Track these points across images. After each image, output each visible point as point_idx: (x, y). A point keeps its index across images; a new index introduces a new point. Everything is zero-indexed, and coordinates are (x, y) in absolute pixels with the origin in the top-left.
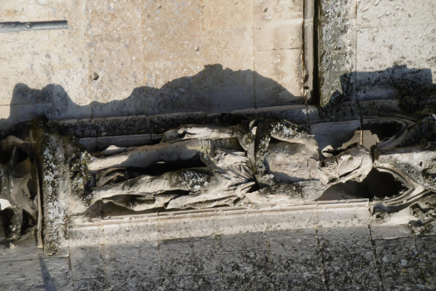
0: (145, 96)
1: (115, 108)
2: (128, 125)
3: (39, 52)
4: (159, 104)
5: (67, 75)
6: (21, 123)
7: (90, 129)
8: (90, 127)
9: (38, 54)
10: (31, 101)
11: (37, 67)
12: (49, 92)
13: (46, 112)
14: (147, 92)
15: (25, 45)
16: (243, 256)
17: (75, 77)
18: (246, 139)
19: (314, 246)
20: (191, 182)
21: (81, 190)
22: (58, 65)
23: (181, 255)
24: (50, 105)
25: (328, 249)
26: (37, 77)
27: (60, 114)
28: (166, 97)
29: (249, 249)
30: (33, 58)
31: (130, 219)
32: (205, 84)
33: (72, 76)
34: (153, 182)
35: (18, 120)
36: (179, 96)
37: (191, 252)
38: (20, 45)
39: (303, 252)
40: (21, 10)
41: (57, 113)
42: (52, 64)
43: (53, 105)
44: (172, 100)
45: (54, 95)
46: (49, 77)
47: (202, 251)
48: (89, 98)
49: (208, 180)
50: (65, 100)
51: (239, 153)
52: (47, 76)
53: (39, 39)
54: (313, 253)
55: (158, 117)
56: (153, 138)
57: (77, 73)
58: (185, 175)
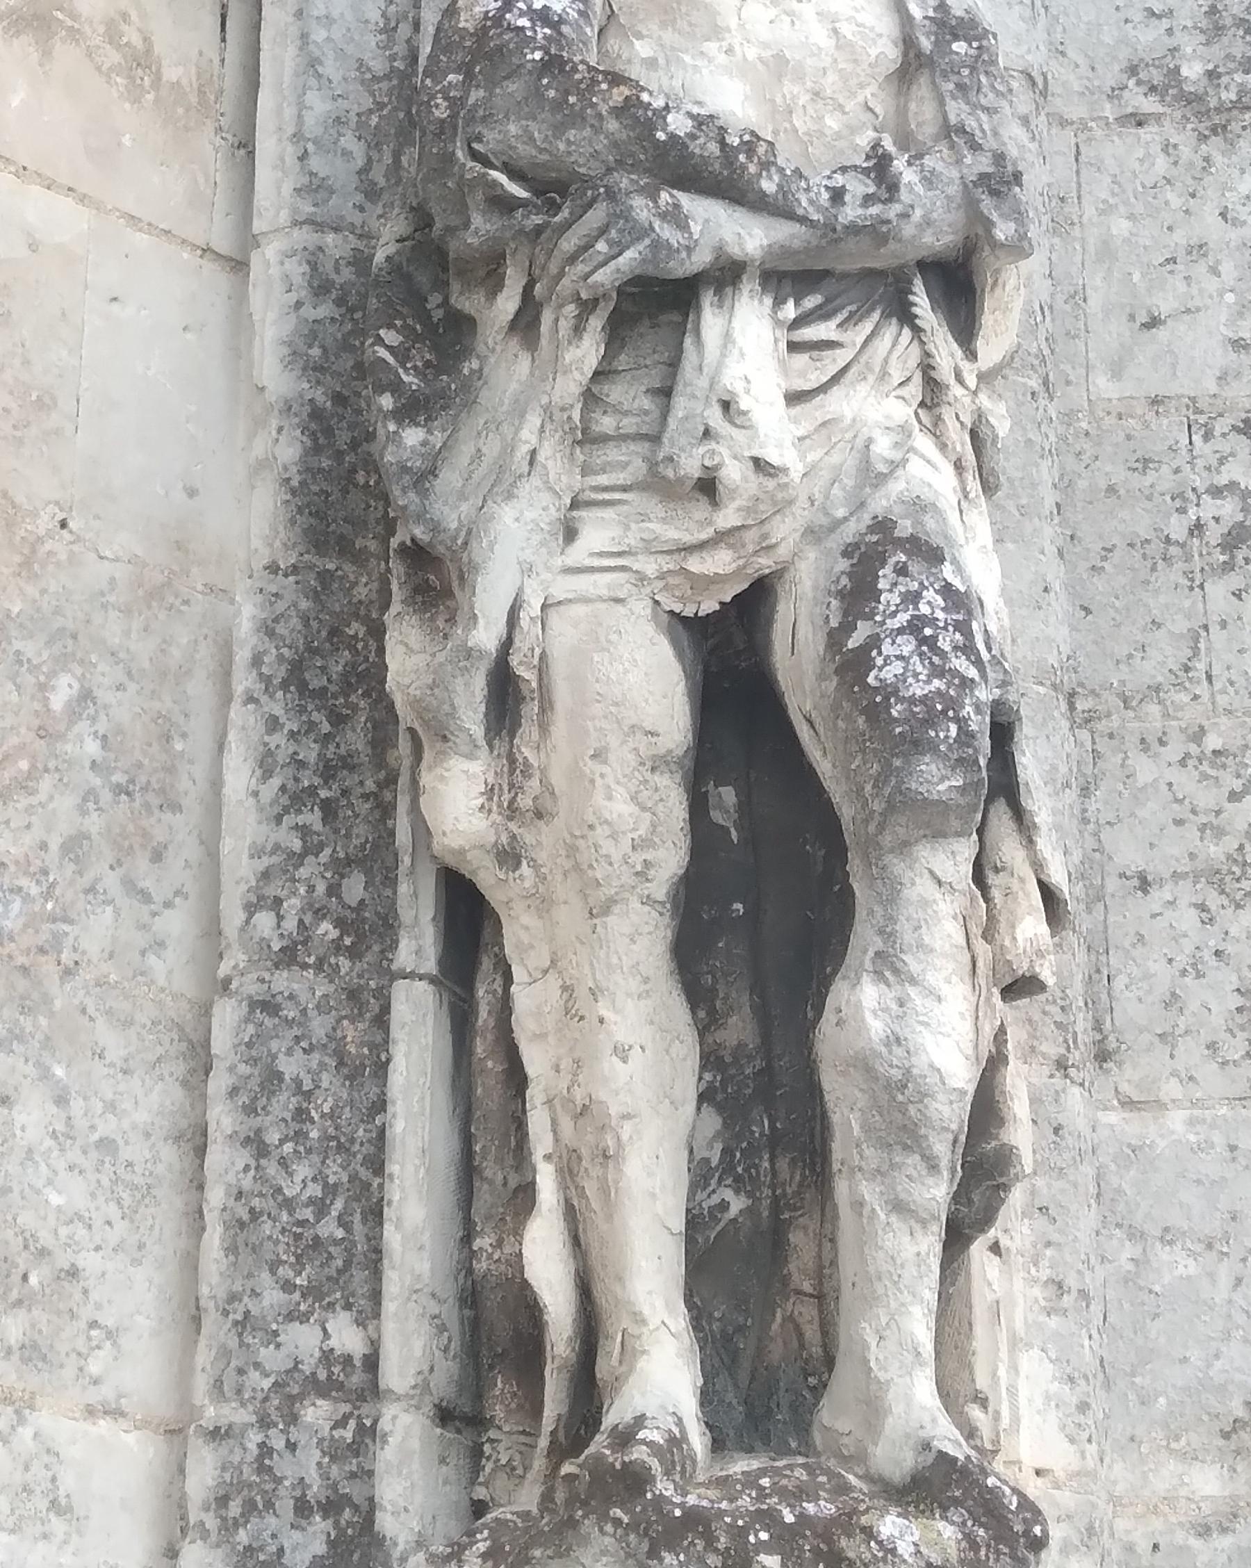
0: (68, 973)
1: (121, 1227)
2: (300, 1136)
4: (129, 885)
7: (292, 1446)
8: (278, 1443)
14: (42, 950)
16: (1228, 567)
18: (663, 216)
19: (1167, 148)
20: (961, 664)
21: (969, 1538)
23: (1212, 961)
25: (1192, 71)
28: (94, 823)
29: (1177, 528)
31: (995, 1248)
32: (45, 522)
34: (912, 963)
36: (102, 726)
37: (1186, 893)
39: (1210, 217)
44: (119, 790)
47: (1179, 822)
48: (21, 1420)
49: (934, 556)
51: (711, 321)
54: (1218, 159)
55: (251, 909)
56: (430, 965)
58: (918, 690)
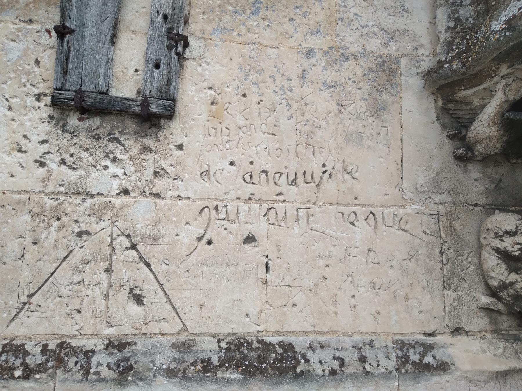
3: (301, 69)
5: (349, 24)
6: (438, 118)
9: (304, 71)
10: (395, 96)
11: (330, 77)
12: (379, 60)
13: (419, 71)
15: (285, 93)
17: (353, 10)
22: (328, 38)
24: (404, 62)
26: (349, 78)
27: (422, 46)
30: (312, 82)
33: (351, 15)
35: (433, 123)
38: (284, 102)
40: (211, 92)
41: (420, 51)
42: (325, 48)
43: (404, 56)
45: (386, 52)
46: (351, 58)
50: (397, 34)
52: (348, 59)
53: (275, 66)
57: (346, 7)
